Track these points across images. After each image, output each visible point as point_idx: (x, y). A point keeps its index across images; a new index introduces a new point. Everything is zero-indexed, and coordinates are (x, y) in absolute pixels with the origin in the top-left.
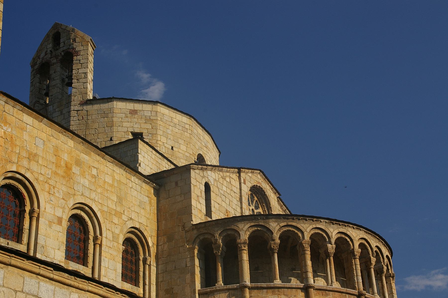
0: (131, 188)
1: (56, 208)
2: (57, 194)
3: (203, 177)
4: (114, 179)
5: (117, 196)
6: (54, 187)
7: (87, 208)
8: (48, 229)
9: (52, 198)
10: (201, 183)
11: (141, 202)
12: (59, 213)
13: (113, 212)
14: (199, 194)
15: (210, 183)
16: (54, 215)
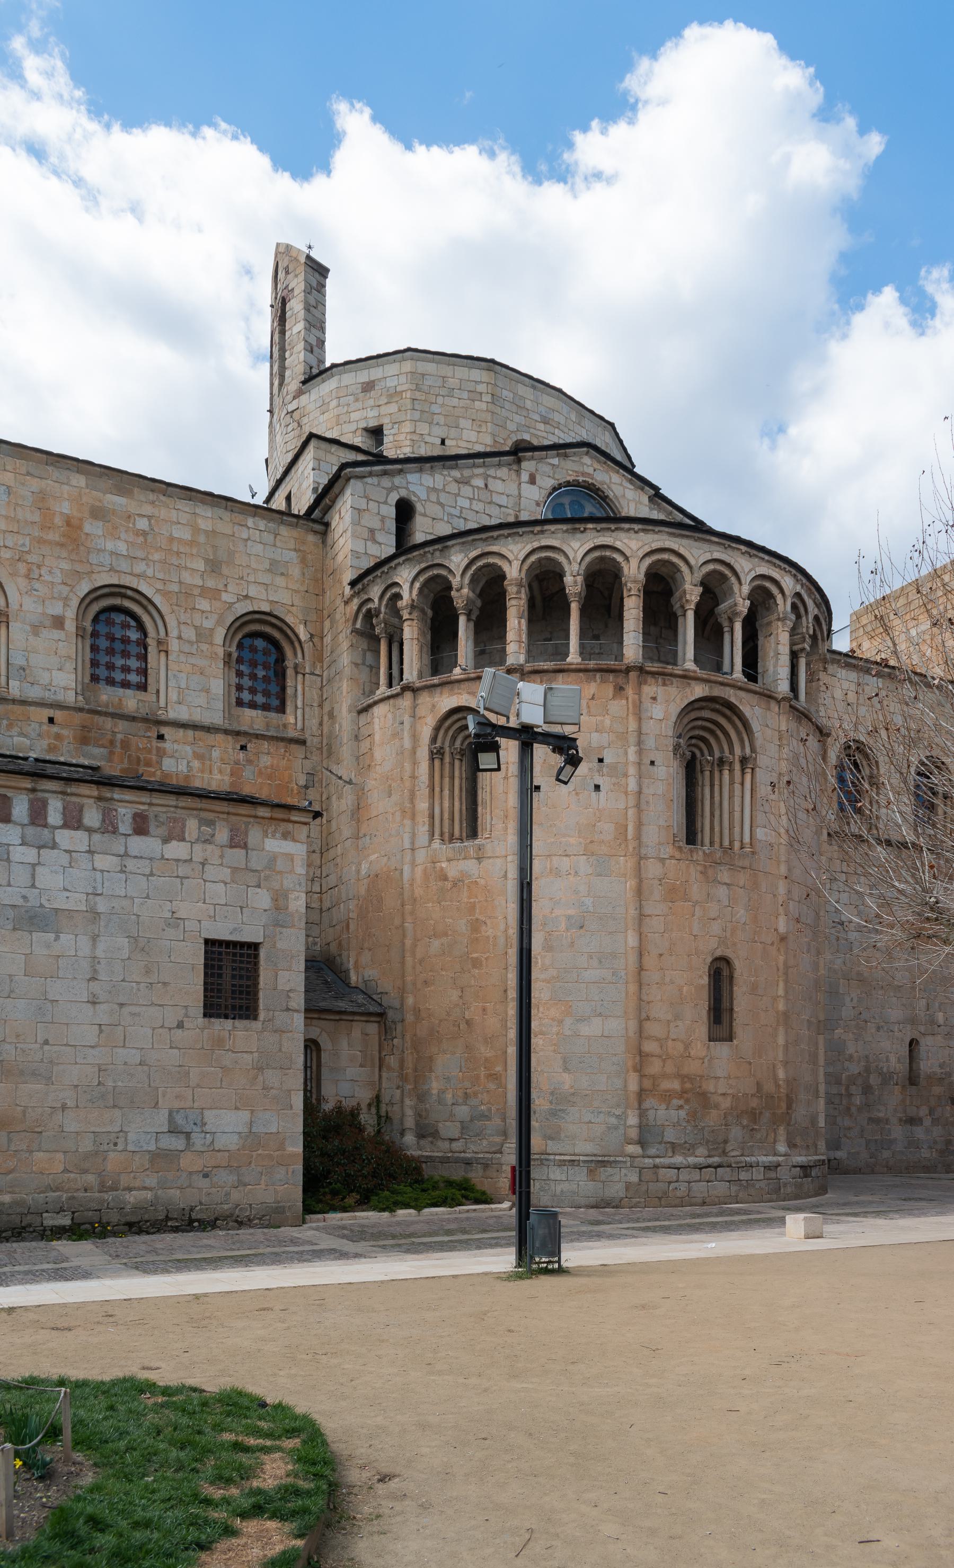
0: (249, 539)
1: (47, 602)
2: (47, 578)
3: (394, 488)
4: (196, 530)
5: (207, 561)
6: (39, 567)
7: (129, 593)
8: (31, 638)
9: (37, 585)
10: (385, 503)
11: (273, 562)
12: (56, 609)
13: (196, 592)
14: (376, 524)
15: (413, 498)
16: (44, 614)
